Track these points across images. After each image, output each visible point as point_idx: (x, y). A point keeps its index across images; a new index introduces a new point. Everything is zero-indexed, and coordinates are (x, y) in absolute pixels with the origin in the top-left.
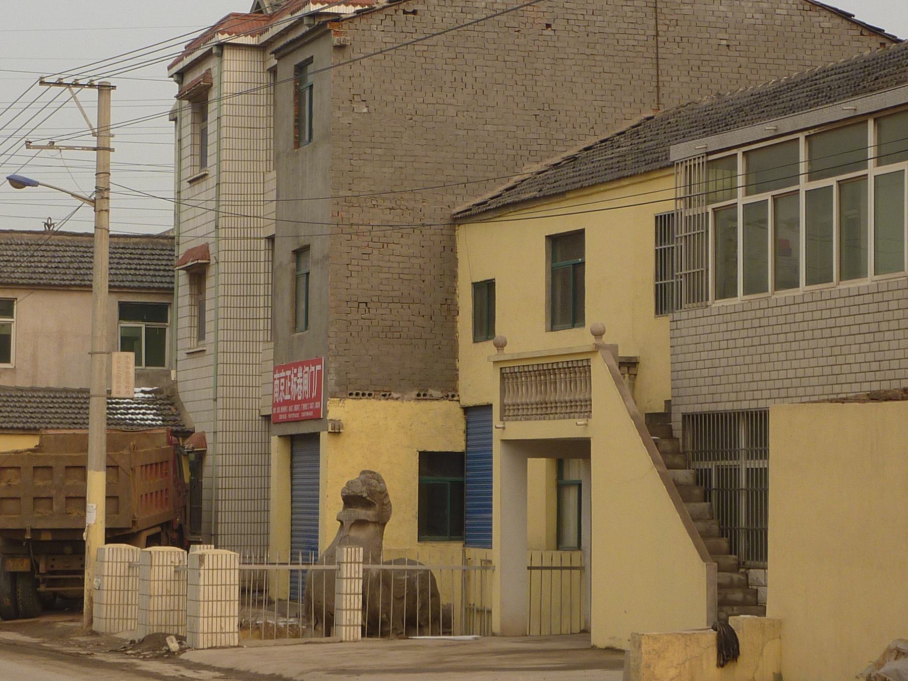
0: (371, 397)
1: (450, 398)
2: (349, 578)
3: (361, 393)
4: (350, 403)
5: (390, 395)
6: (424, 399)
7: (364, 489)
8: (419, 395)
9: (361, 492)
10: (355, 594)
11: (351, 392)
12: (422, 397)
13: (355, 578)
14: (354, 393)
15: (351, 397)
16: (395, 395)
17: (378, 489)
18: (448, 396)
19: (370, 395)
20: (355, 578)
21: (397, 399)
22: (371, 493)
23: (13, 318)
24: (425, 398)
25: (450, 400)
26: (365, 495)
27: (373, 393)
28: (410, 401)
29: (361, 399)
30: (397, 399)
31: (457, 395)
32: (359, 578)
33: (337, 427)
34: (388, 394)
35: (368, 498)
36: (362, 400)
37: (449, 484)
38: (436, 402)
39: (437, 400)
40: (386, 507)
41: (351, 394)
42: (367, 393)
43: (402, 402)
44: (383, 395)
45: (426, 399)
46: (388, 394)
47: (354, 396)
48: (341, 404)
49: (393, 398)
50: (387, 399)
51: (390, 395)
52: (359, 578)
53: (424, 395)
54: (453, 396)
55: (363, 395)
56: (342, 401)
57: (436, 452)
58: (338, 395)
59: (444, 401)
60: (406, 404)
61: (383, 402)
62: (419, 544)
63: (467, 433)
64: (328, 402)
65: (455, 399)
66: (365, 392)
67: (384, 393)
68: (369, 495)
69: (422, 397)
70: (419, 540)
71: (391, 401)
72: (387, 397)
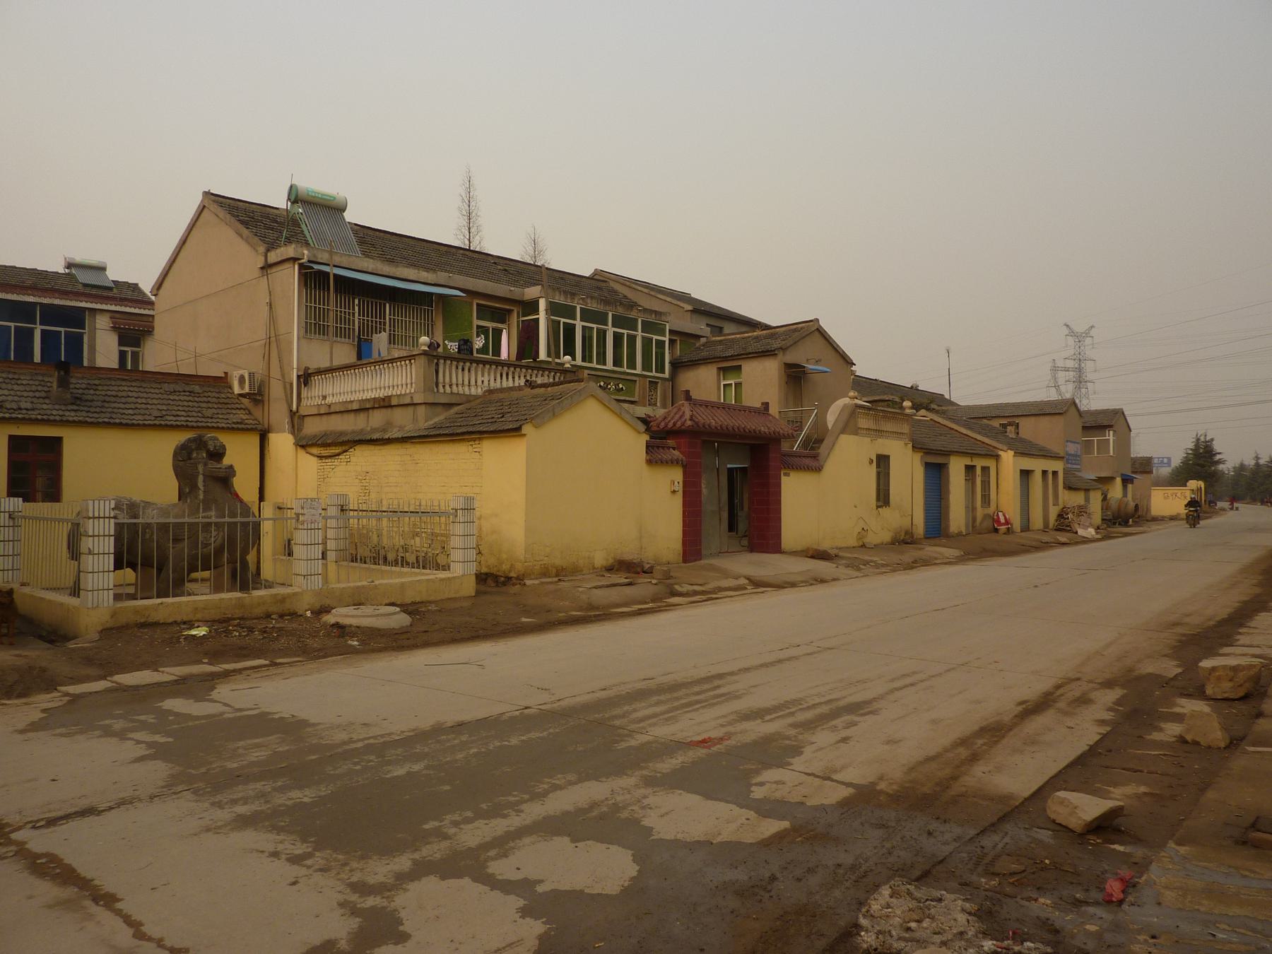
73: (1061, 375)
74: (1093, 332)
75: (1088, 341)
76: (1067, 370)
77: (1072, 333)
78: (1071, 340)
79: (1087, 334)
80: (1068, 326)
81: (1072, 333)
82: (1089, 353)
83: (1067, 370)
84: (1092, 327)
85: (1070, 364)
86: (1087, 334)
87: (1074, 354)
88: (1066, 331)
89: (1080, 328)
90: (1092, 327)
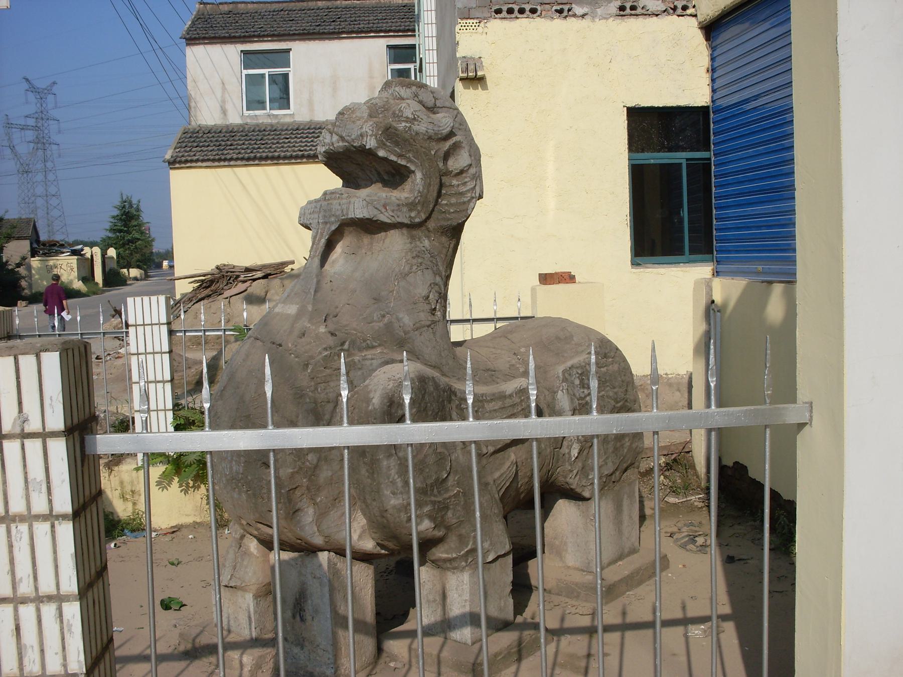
0: (535, 15)
1: (679, 11)
2: (21, 518)
3: (516, 8)
4: (497, 26)
5: (569, 10)
6: (631, 15)
7: (367, 128)
8: (622, 8)
9: (362, 135)
10: (39, 599)
11: (497, 7)
12: (628, 11)
13: (30, 518)
14: (505, 8)
15: (496, 16)
16: (578, 10)
17: (421, 128)
18: (675, 9)
19: (533, 11)
20: (30, 518)
21: (583, 16)
22: (389, 134)
23: (290, 67)
24: (633, 12)
25: (679, 16)
26: (371, 143)
27: (539, 8)
28: (607, 19)
29: (517, 18)
30: (583, 16)
31: (690, 5)
32: (51, 517)
33: (471, 67)
34: (566, 8)
35: (381, 153)
36: (518, 21)
37: (684, 163)
38: (655, 18)
39: (657, 15)
40: (455, 182)
41: (498, 11)
42: (527, 7)
43: (593, 21)
44: (556, 11)
45: (637, 15)
46: (566, 8)
47: (504, 14)
48: (480, 29)
49: (575, 16)
50: (565, 17)
51: (569, 10)
52: (51, 517)
53: (633, 8)
54: (685, 8)
55: (521, 11)
56: (482, 24)
57: (658, 108)
58: (473, 13)
59: (670, 17)
60: (600, 24)
61: (558, 24)
62: (634, 270)
63: (713, 70)
64: (458, 27)
65: (689, 12)
66: (523, 6)
67: (558, 8)
68: (382, 145)
69: (628, 11)
70: (634, 264)
71: (573, 19)
72: (565, 13)
73: (17, 135)
74: (55, 89)
75: (50, 98)
76: (23, 128)
77: (33, 89)
78: (31, 97)
79: (49, 90)
80: (27, 80)
81: (33, 89)
82: (54, 113)
83: (23, 128)
84: (54, 83)
85: (31, 122)
86: (49, 90)
87: (36, 113)
88: (26, 86)
89: (41, 84)
90: (54, 83)
